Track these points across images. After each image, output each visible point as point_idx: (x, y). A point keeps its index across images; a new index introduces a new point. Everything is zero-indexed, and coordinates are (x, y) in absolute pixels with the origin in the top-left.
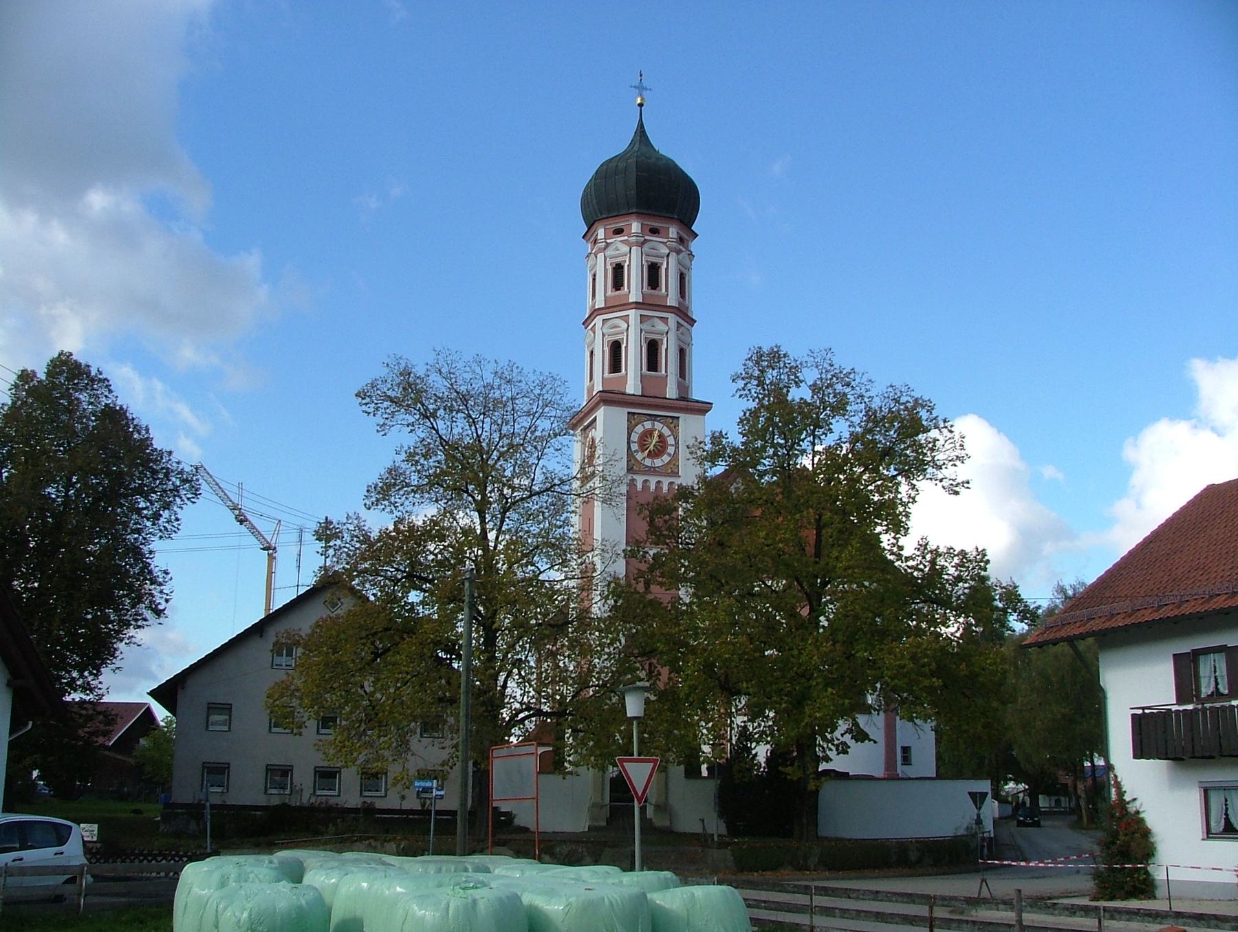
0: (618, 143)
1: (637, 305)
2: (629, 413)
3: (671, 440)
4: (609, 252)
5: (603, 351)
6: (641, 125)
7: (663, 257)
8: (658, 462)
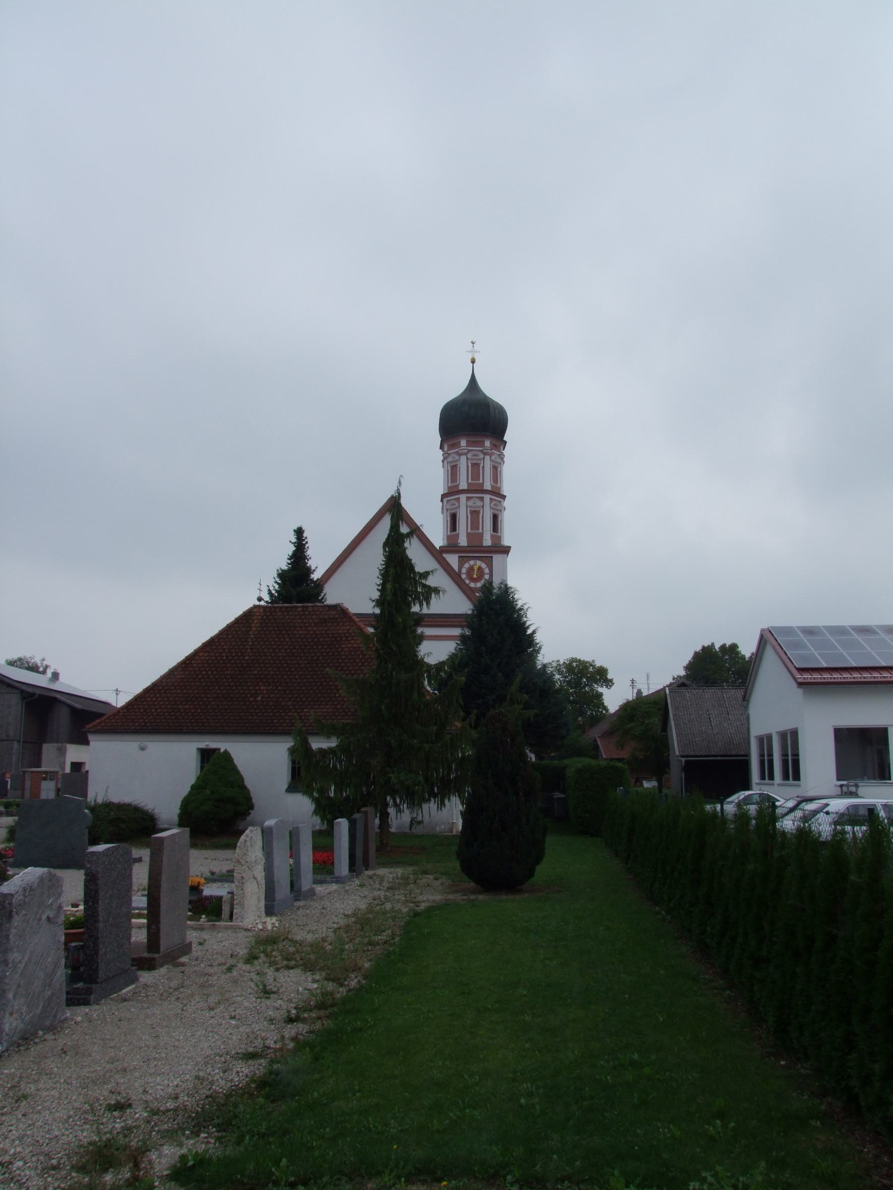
3: (487, 571)
4: (469, 456)
5: (467, 516)
6: (473, 376)
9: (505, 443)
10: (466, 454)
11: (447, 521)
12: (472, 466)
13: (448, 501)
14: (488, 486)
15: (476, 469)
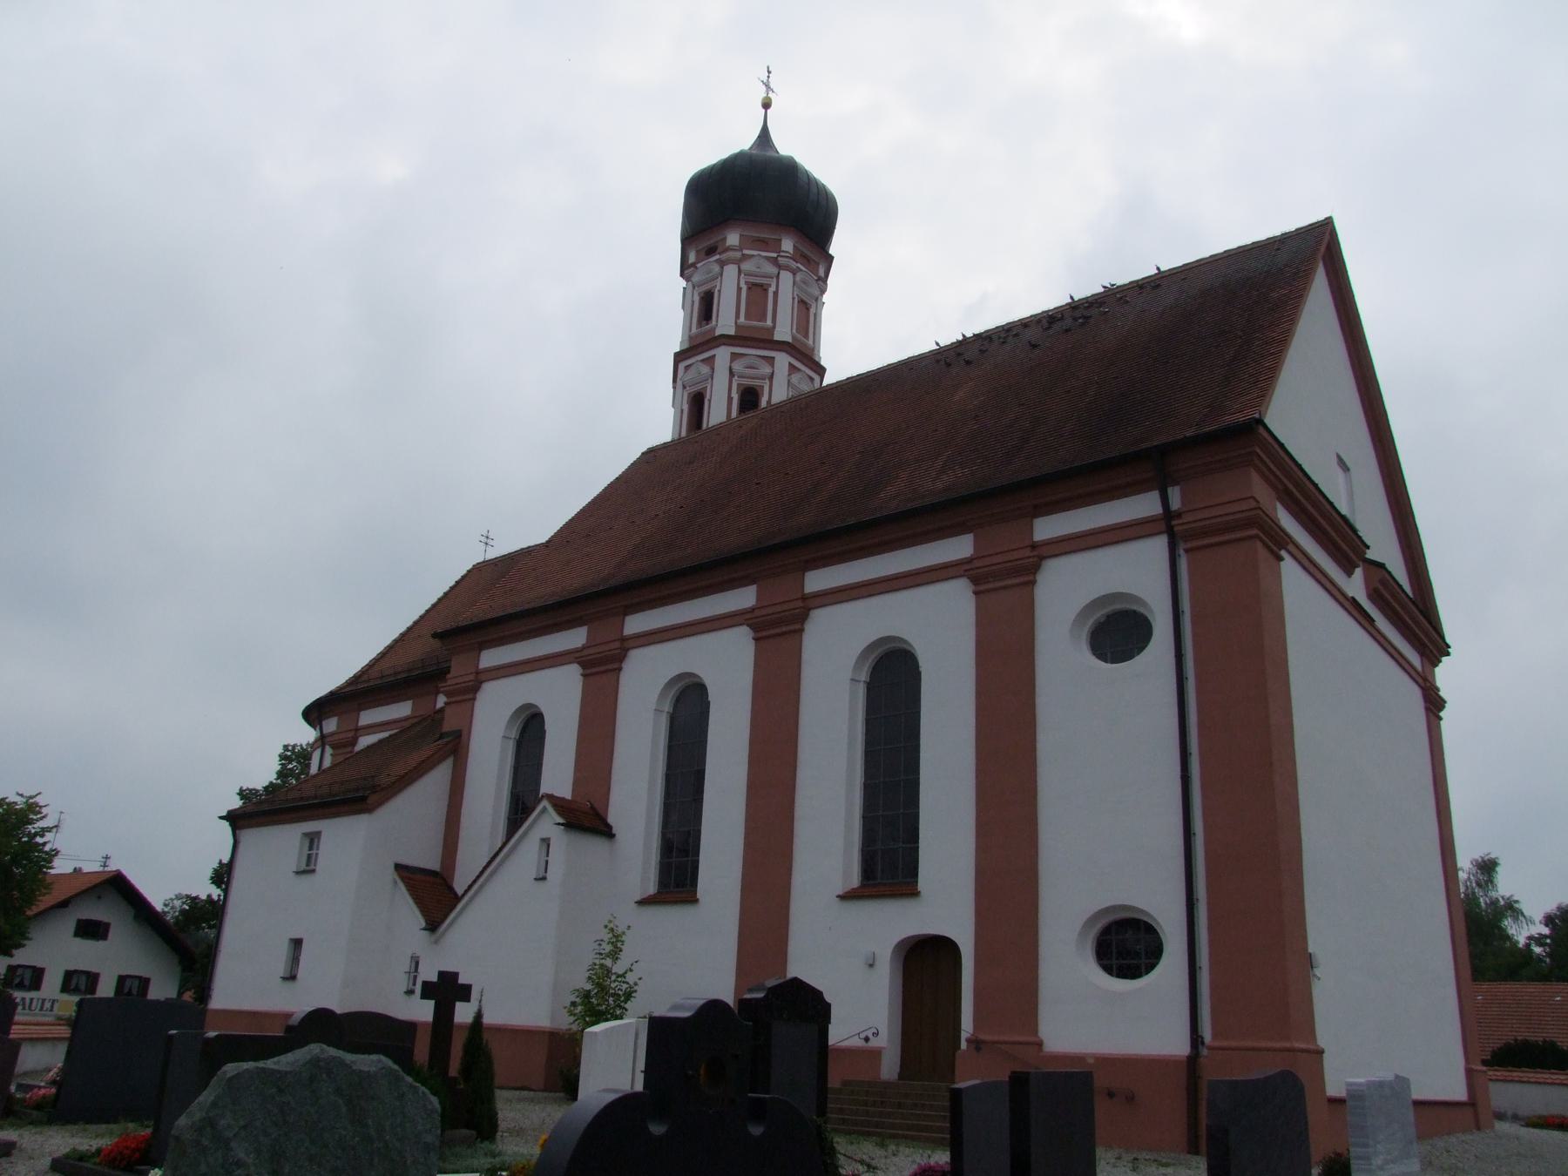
0: (742, 140)
4: (746, 266)
5: (730, 399)
9: (830, 259)
10: (738, 262)
11: (682, 411)
12: (749, 289)
13: (687, 368)
14: (784, 331)
15: (757, 293)
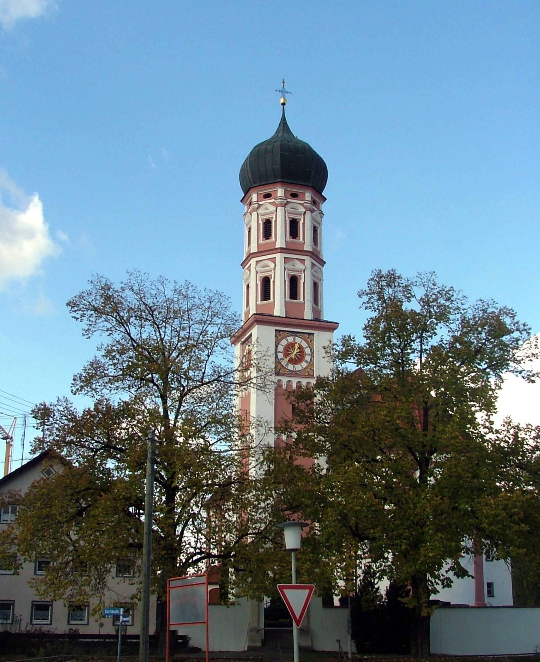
1: (282, 250)
2: (276, 330)
3: (308, 351)
4: (261, 211)
5: (257, 284)
6: (284, 119)
7: (301, 215)
8: (298, 367)
